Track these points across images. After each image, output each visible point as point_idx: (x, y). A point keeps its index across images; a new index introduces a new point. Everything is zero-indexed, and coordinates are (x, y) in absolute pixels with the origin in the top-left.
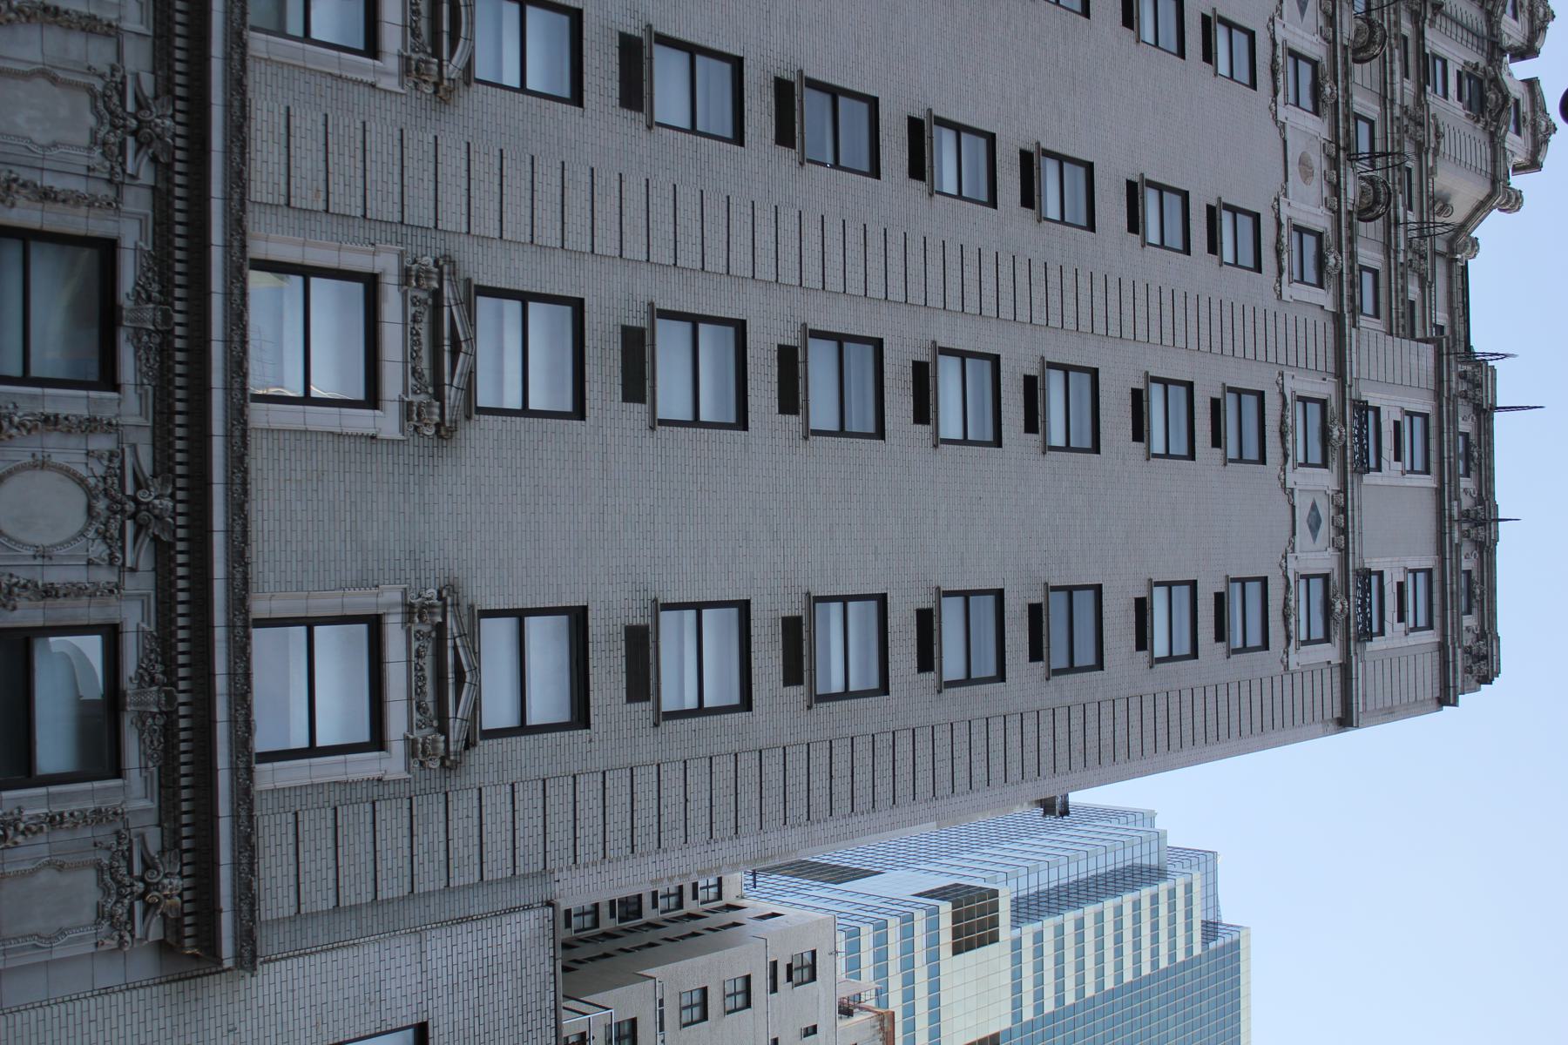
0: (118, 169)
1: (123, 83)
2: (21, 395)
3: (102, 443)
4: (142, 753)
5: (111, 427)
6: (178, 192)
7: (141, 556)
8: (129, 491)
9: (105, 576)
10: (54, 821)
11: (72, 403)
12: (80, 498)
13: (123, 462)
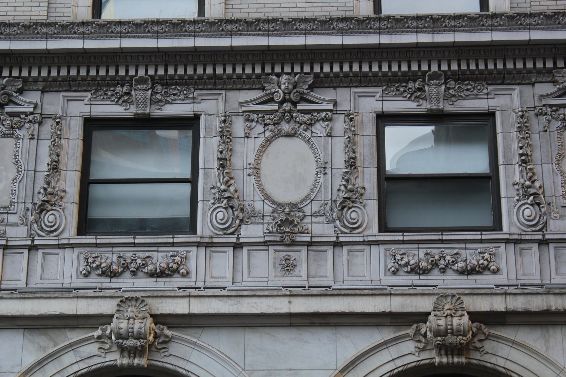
0: (31, 117)
2: (205, 184)
3: (239, 126)
4: (476, 97)
5: (226, 120)
6: (44, 73)
7: (325, 97)
9: (340, 124)
10: (525, 160)
11: (210, 149)
12: (281, 142)
13: (253, 112)
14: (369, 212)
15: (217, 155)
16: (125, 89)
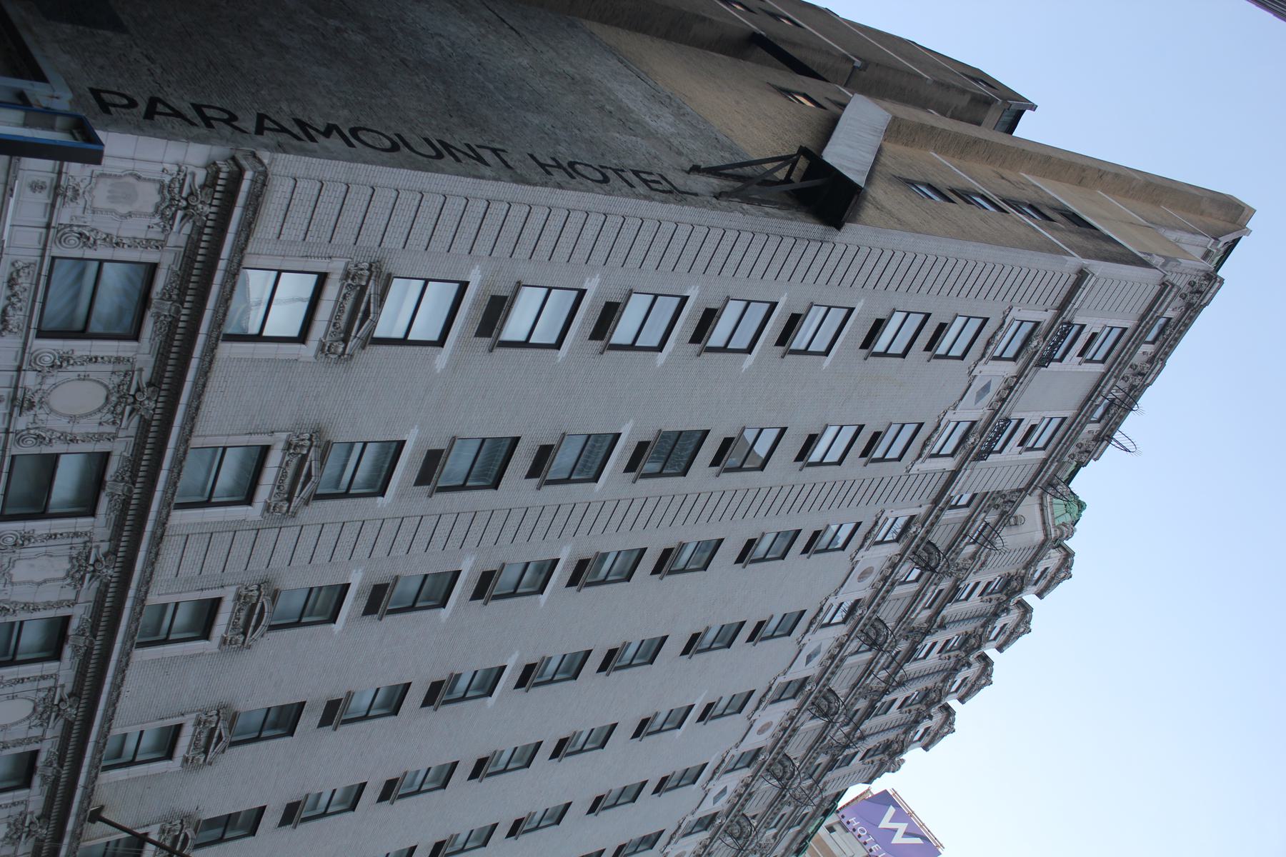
1: (184, 180)
6: (183, 318)
8: (132, 392)
12: (104, 393)
15: (101, 354)
16: (175, 297)
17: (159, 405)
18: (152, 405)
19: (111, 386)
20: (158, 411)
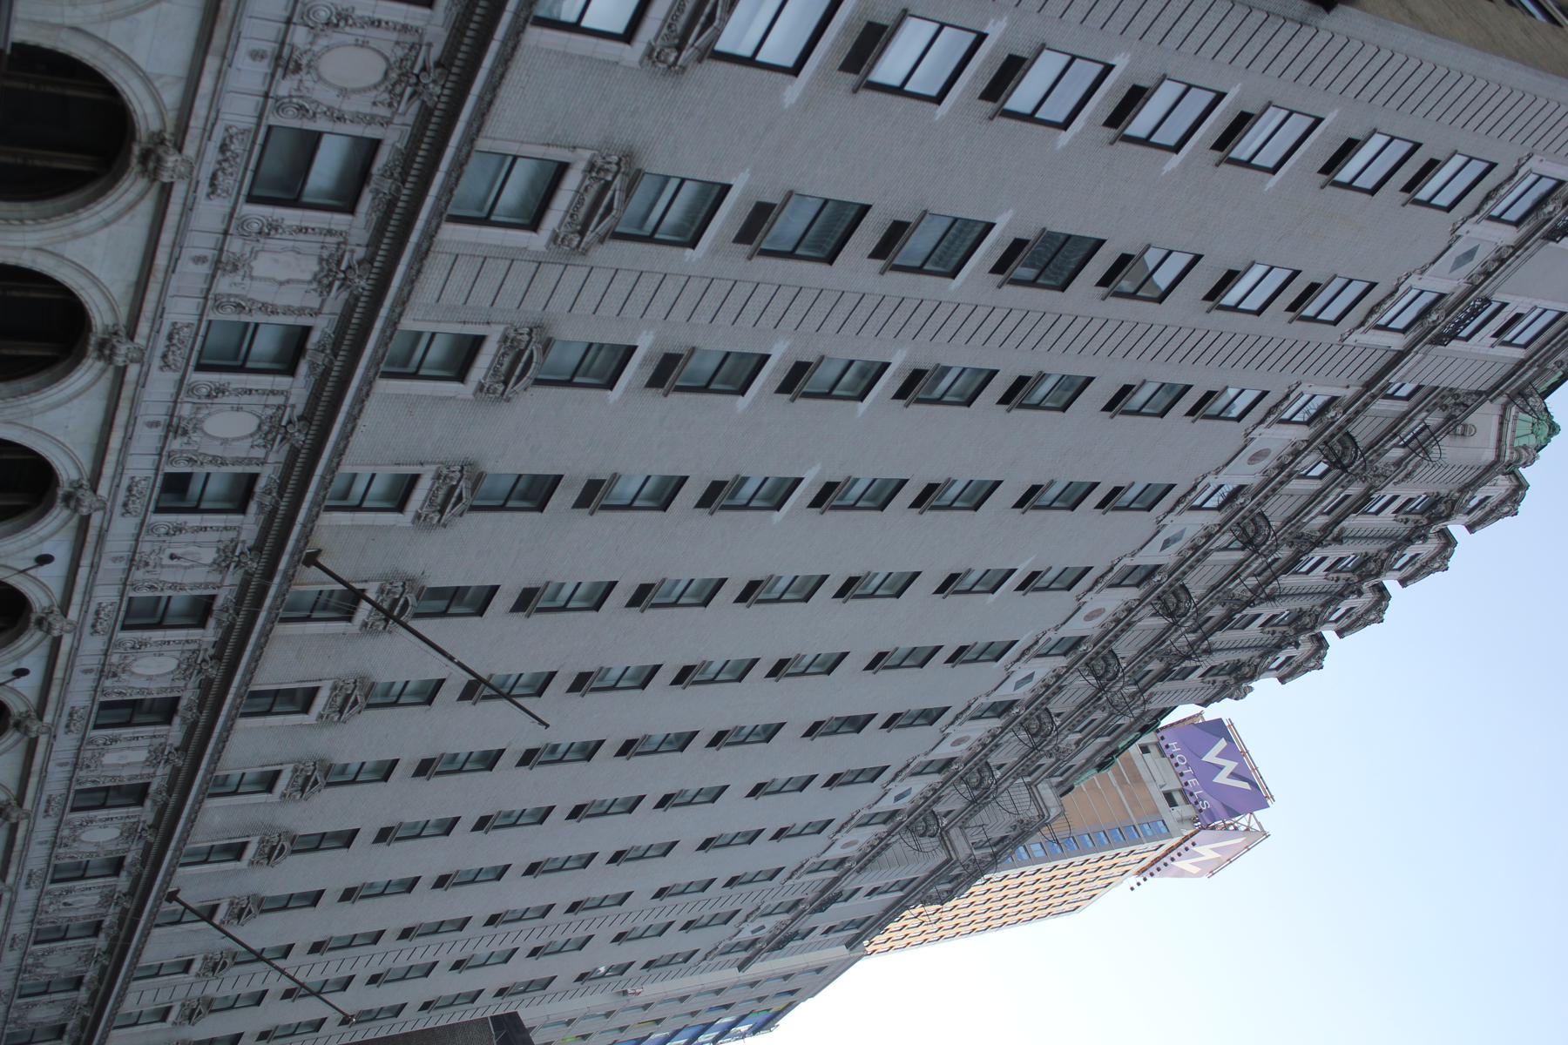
9: (383, 111)
10: (303, 230)
12: (382, 66)
14: (290, 120)
15: (385, 18)
17: (446, 92)
18: (438, 90)
19: (392, 60)
20: (443, 99)
